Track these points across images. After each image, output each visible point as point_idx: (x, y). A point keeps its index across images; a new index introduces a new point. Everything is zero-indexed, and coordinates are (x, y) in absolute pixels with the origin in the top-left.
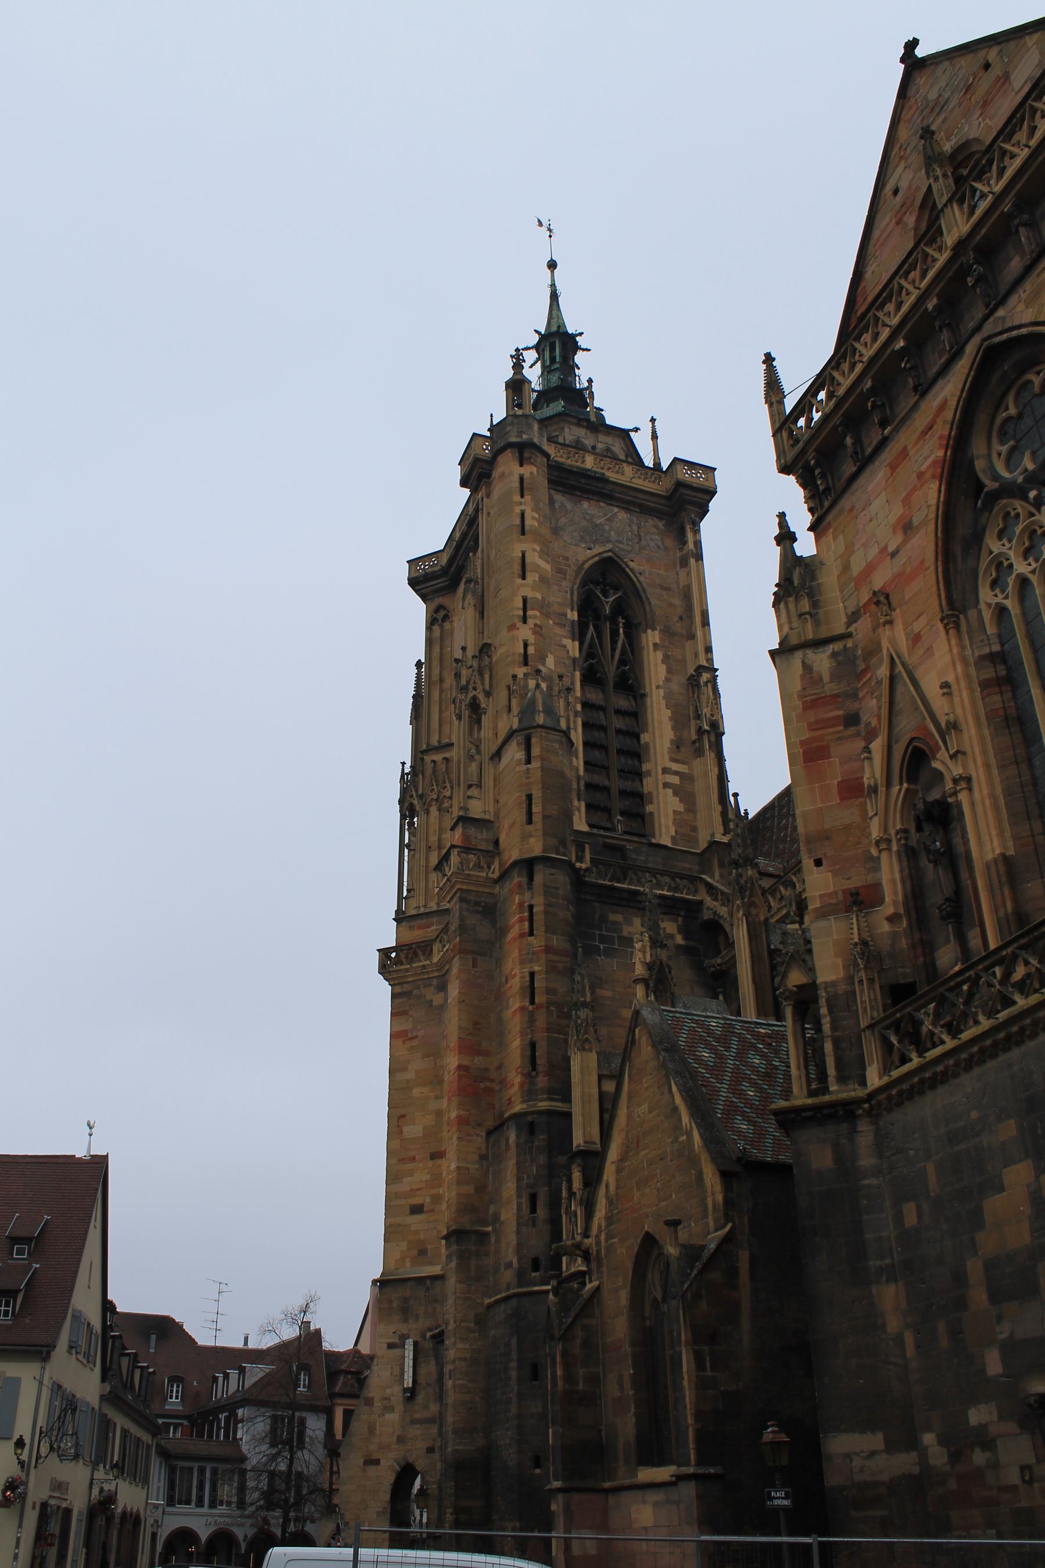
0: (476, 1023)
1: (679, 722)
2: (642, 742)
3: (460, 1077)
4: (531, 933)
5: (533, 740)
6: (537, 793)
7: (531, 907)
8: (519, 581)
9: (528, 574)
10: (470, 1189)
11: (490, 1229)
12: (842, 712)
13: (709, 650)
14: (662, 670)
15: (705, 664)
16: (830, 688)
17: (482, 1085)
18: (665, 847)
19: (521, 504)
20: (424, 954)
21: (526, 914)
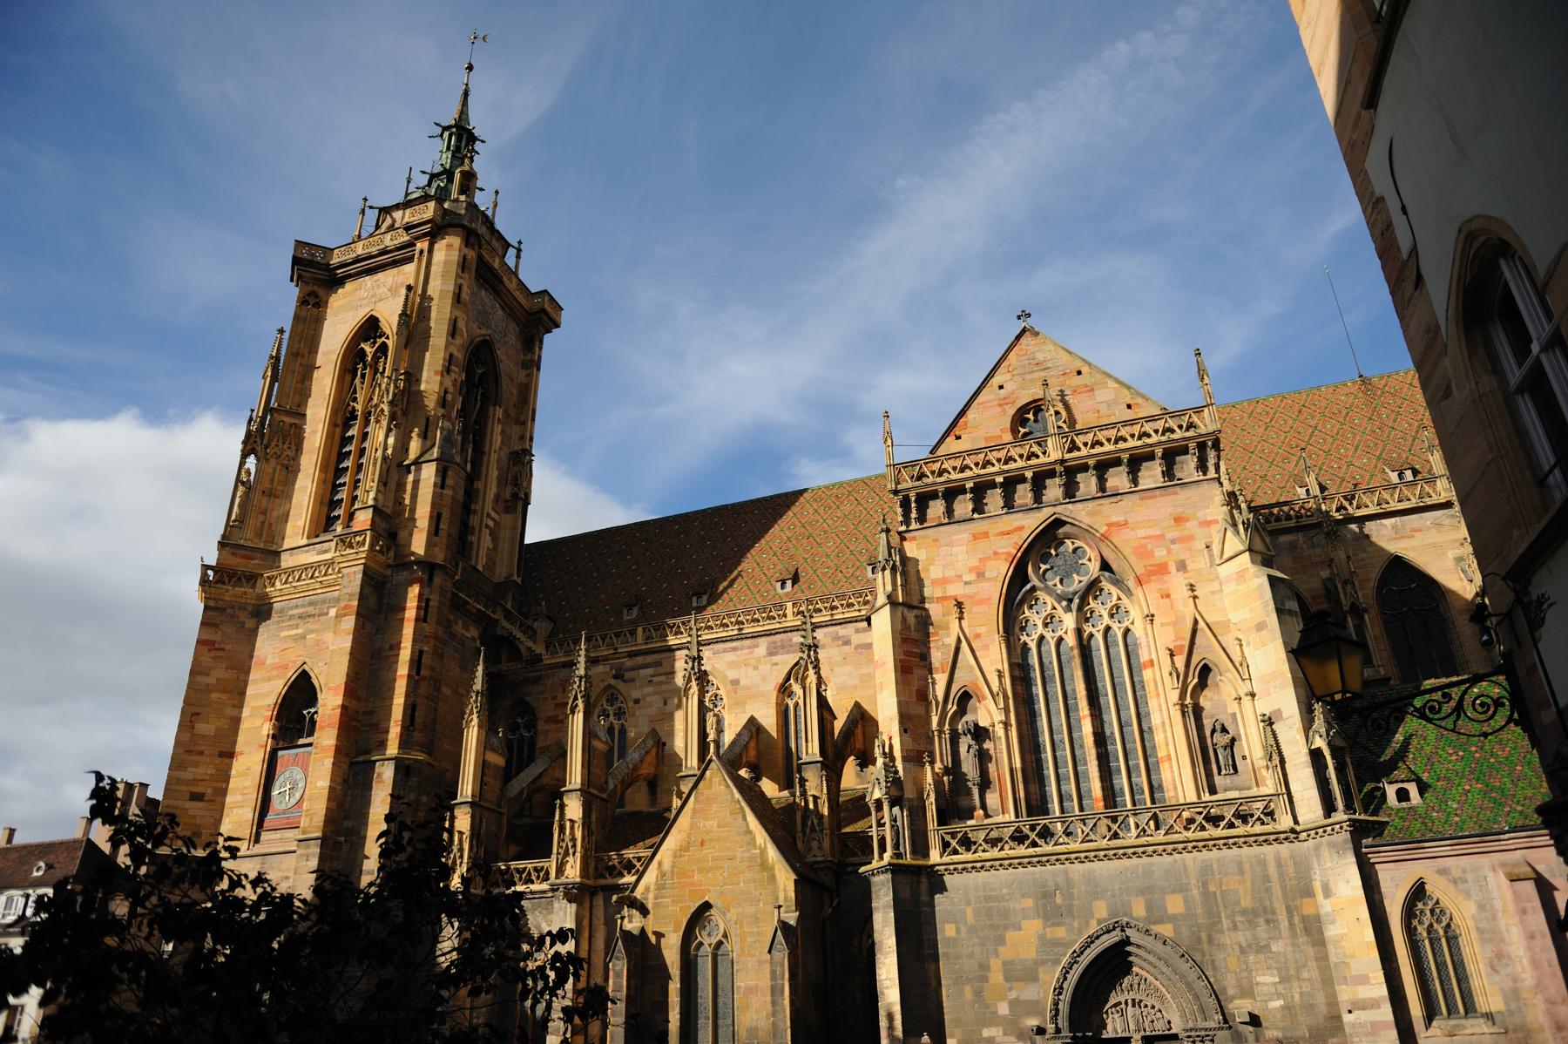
0: (357, 674)
1: (502, 483)
2: (475, 486)
3: (342, 714)
4: (425, 620)
5: (449, 473)
6: (446, 514)
7: (428, 600)
8: (450, 339)
9: (457, 337)
10: (334, 805)
11: (342, 839)
12: (917, 651)
13: (531, 439)
14: (499, 439)
15: (528, 447)
16: (914, 635)
17: (353, 724)
18: (478, 570)
19: (461, 278)
20: (248, 581)
21: (424, 604)
